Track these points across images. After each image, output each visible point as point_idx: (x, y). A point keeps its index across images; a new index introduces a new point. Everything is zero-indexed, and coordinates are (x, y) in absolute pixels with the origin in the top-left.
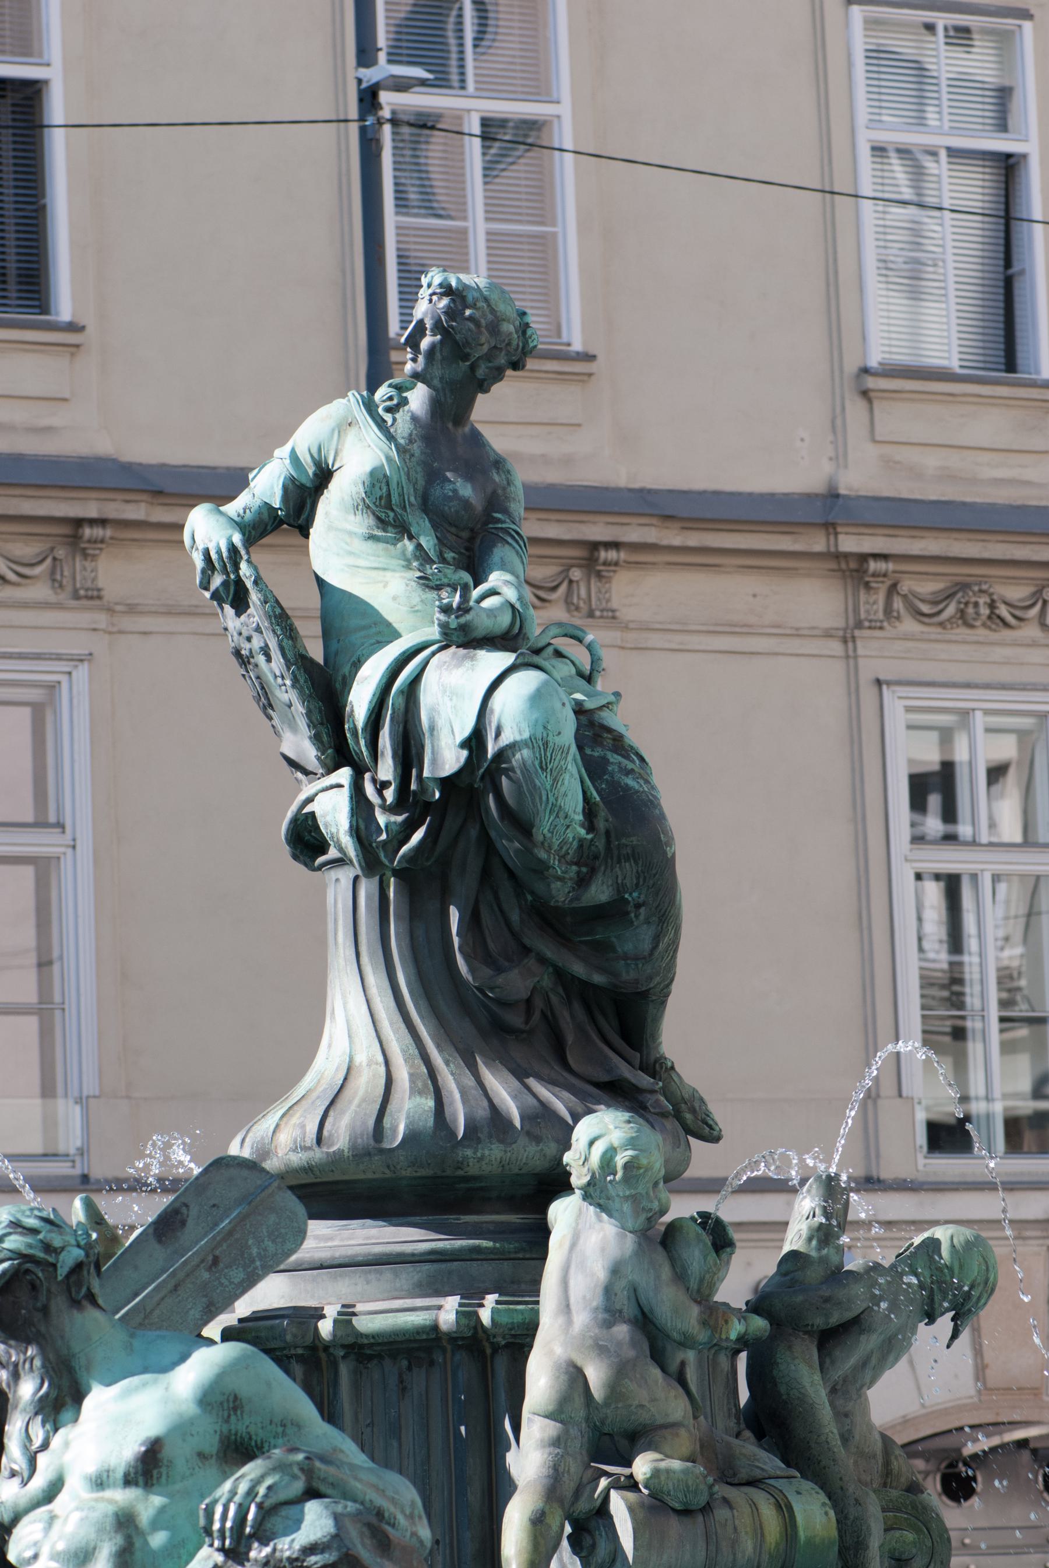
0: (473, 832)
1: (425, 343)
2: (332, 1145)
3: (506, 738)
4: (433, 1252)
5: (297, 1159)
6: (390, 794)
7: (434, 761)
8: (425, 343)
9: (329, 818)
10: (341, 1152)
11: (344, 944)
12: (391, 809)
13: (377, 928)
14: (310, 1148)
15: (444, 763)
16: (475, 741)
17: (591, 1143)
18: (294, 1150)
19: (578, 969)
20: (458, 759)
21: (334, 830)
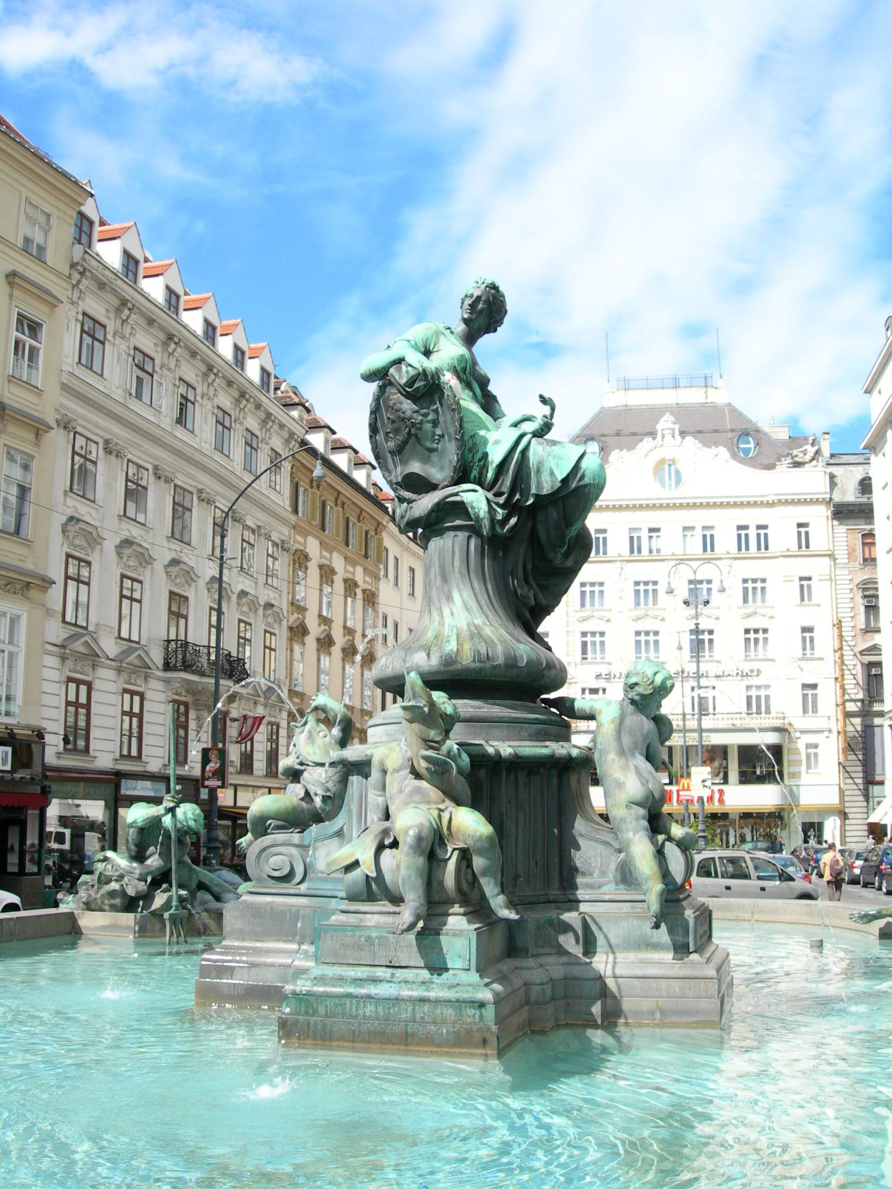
0: (530, 524)
1: (480, 306)
2: (494, 661)
3: (587, 480)
4: (536, 719)
5: (473, 665)
6: (501, 500)
7: (539, 486)
8: (480, 306)
9: (474, 504)
10: (498, 666)
11: (460, 567)
12: (502, 506)
13: (479, 561)
14: (484, 662)
15: (543, 488)
16: (565, 481)
17: (655, 674)
18: (474, 661)
19: (540, 596)
20: (552, 487)
21: (476, 510)
